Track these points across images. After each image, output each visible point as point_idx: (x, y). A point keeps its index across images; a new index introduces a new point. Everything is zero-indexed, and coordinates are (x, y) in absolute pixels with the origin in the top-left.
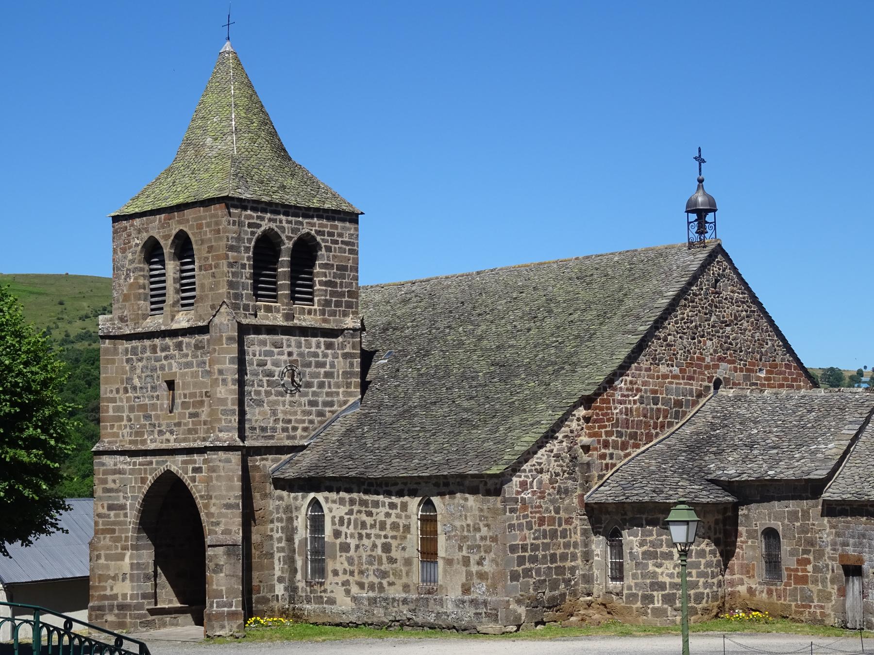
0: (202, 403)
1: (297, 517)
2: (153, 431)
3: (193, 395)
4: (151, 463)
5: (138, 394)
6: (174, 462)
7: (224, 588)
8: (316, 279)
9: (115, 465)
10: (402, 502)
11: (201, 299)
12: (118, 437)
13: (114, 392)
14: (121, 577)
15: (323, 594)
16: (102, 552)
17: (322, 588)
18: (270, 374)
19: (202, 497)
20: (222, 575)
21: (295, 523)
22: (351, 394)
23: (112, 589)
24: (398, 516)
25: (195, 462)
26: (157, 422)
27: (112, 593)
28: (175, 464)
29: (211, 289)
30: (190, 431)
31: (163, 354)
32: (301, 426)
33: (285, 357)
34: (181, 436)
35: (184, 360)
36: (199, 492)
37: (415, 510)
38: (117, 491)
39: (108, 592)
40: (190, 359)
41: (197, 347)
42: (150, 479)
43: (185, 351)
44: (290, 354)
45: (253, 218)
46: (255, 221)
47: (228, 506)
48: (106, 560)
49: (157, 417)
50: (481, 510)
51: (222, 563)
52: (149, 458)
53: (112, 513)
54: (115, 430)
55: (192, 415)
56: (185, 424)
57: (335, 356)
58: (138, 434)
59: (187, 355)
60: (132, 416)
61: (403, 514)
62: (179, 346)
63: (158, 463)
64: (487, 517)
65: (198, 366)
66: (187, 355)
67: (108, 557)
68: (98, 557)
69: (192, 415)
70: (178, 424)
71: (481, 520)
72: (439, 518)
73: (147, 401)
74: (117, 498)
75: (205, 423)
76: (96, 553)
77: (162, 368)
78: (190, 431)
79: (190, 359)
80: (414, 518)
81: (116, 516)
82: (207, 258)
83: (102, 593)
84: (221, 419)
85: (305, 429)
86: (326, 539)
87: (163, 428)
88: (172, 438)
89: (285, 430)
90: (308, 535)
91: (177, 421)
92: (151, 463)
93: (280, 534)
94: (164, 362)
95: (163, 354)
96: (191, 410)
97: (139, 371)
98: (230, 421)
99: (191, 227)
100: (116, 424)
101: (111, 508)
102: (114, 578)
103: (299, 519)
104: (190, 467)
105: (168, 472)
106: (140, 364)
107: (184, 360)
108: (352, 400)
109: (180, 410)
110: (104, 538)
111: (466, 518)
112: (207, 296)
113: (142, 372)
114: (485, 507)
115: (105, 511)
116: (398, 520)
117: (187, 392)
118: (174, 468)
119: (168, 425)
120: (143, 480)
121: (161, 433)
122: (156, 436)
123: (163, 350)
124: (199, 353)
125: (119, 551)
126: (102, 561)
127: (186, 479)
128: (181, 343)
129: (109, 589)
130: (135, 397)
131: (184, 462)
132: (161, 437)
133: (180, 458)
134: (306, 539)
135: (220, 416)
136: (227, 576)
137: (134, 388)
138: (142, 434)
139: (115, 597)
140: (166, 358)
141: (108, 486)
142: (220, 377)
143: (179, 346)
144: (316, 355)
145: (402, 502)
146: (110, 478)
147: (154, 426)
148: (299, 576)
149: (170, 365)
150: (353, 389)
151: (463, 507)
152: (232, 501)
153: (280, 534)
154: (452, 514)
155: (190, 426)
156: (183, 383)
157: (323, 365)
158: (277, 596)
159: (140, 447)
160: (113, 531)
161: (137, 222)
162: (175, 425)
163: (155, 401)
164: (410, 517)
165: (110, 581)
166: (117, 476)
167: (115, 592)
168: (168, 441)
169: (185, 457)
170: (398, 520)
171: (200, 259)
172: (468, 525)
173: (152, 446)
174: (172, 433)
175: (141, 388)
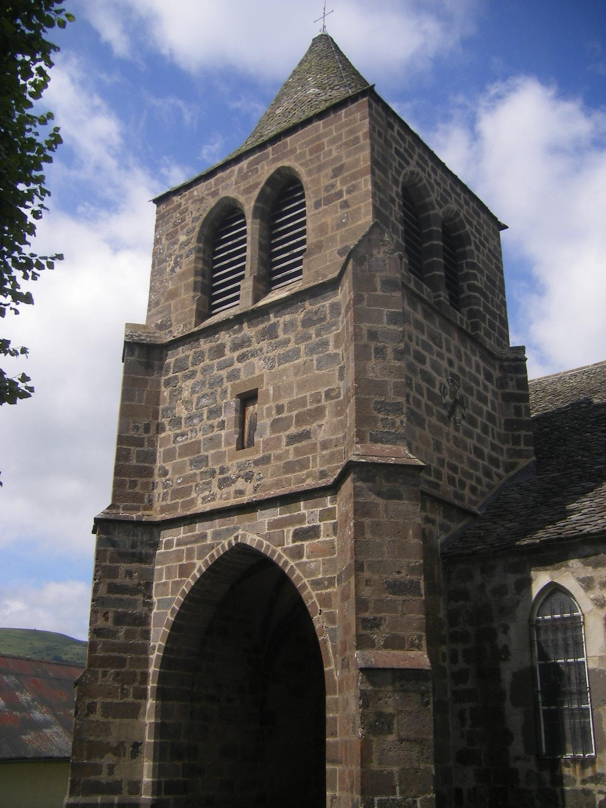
0: (318, 413)
1: (506, 629)
2: (209, 483)
3: (302, 402)
4: (204, 537)
5: (184, 429)
6: (252, 529)
7: (395, 769)
8: (465, 285)
9: (134, 546)
11: (319, 246)
12: (142, 501)
13: (141, 430)
14: (129, 749)
15: (590, 786)
16: (99, 700)
17: (589, 772)
18: (430, 380)
19: (316, 584)
20: (391, 738)
21: (501, 640)
22: (520, 454)
23: (111, 769)
25: (301, 519)
26: (217, 467)
27: (110, 779)
28: (254, 532)
29: (340, 225)
30: (289, 467)
31: (236, 354)
32: (468, 482)
33: (444, 364)
34: (268, 480)
35: (280, 351)
36: (312, 573)
38: (134, 591)
39: (104, 777)
40: (292, 346)
41: (307, 323)
42: (200, 565)
43: (282, 336)
44: (451, 363)
45: (401, 146)
46: (402, 150)
47: (396, 587)
48: (105, 714)
49: (220, 457)
51: (390, 710)
52: (199, 528)
53: (122, 630)
54: (137, 489)
55: (292, 439)
56: (279, 458)
57: (495, 394)
58: (177, 493)
59: (287, 342)
60: (168, 466)
62: (270, 333)
63: (217, 535)
65: (311, 351)
66: (287, 342)
67: (108, 710)
68: (91, 709)
69: (292, 439)
70: (265, 460)
73: (200, 436)
74: (133, 604)
75: (325, 445)
76: (88, 701)
77: (233, 376)
78: (289, 467)
79: (292, 346)
81: (128, 634)
82: (333, 186)
83: (92, 778)
84: (375, 419)
85: (473, 490)
86: (591, 665)
87: (231, 474)
88: (249, 487)
89: (451, 481)
90: (537, 663)
91: (261, 455)
92: (204, 537)
93: (462, 664)
94: (238, 365)
95: (236, 354)
96: (293, 430)
97: (186, 394)
98: (393, 424)
99: (297, 159)
100: (140, 481)
101: (120, 619)
102: (118, 750)
103: (512, 632)
104: (289, 531)
105: (242, 550)
106: (190, 383)
107: (280, 351)
108: (523, 463)
109: (268, 434)
110: (105, 674)
112: (332, 239)
113: (193, 392)
115: (110, 624)
117: (285, 401)
118: (252, 539)
119: (241, 467)
120: (184, 571)
121: (225, 483)
122: (215, 489)
123: (235, 348)
124: (312, 331)
125: (131, 699)
126: (97, 716)
127: (280, 555)
128: (274, 327)
129: (105, 771)
130: (177, 436)
131: (272, 525)
132: (225, 490)
133: (265, 517)
134: (533, 669)
135: (375, 413)
136: (401, 740)
137: (176, 422)
138: (185, 492)
139: (114, 788)
140: (241, 358)
141: (118, 581)
142: (373, 345)
143: (270, 333)
144: (477, 382)
146: (123, 567)
147: (213, 473)
148: (517, 747)
149: (252, 367)
150: (522, 447)
152: (405, 576)
153: (462, 664)
155: (291, 457)
156: (277, 389)
157: (483, 399)
158: (458, 792)
159: (180, 513)
160: (121, 662)
161: (197, 191)
162: (257, 463)
163: (216, 432)
165: (110, 755)
166: (135, 565)
167: (117, 776)
168: (240, 493)
169: (276, 514)
171: (316, 193)
173: (208, 507)
174: (248, 477)
175: (190, 418)
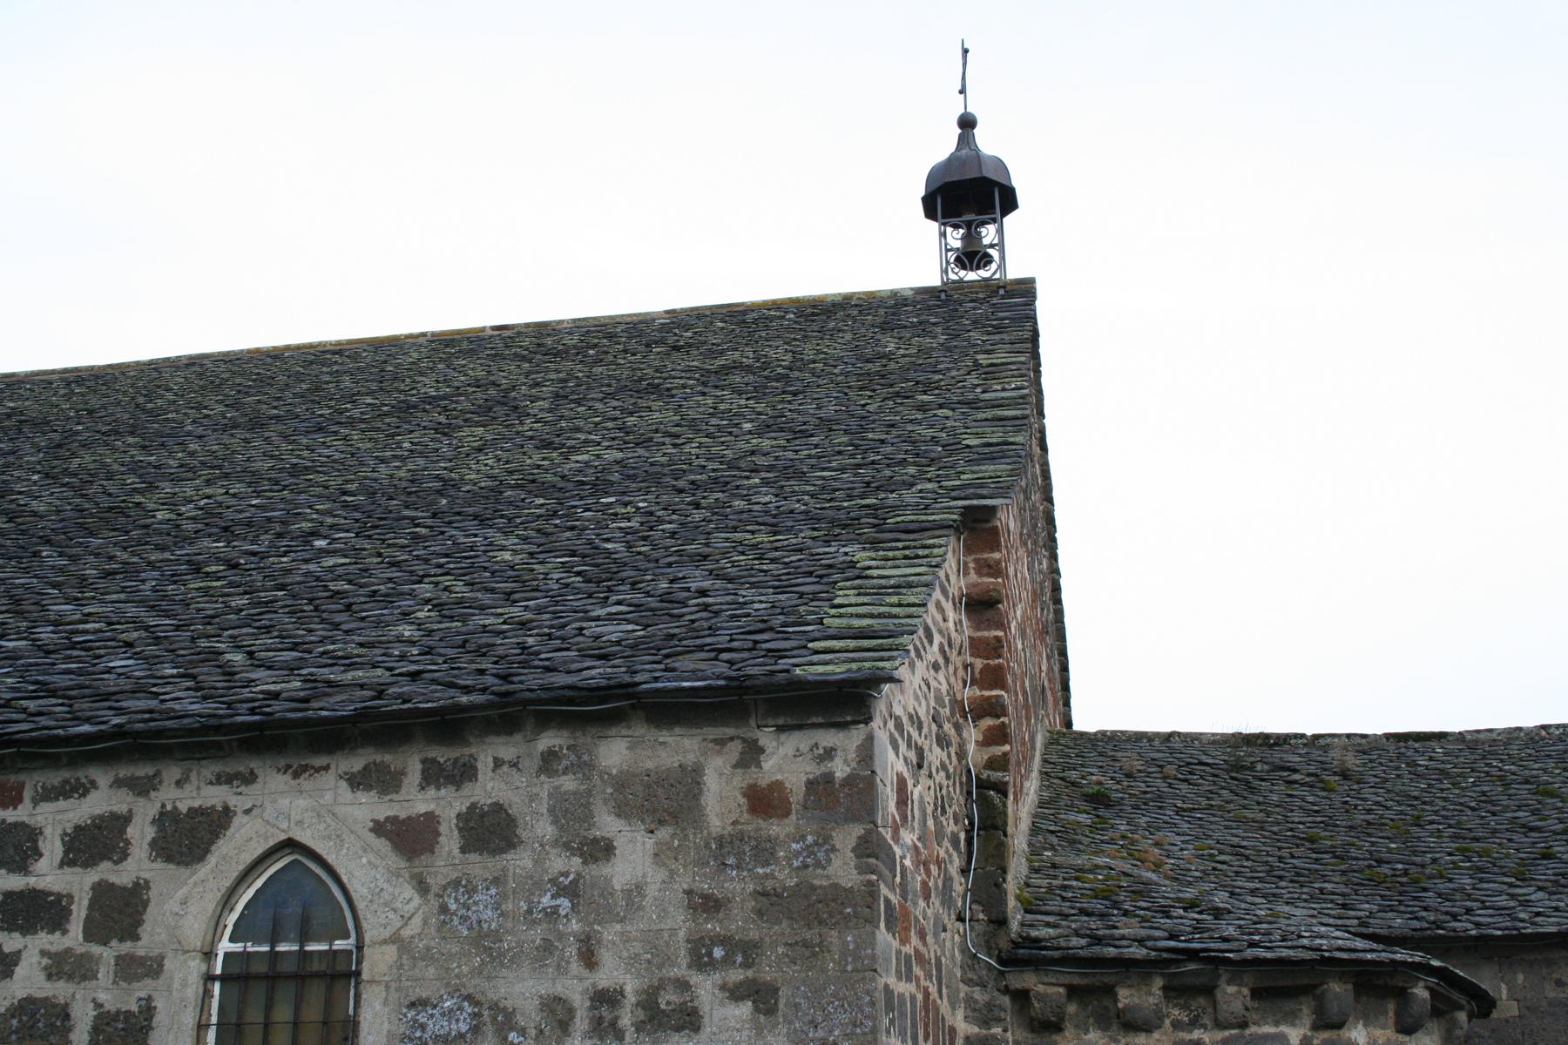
10: (102, 891)
24: (61, 966)
37: (194, 930)
50: (706, 905)
61: (107, 954)
64: (748, 951)
71: (701, 961)
72: (378, 962)
80: (185, 975)
111: (589, 959)
114: (737, 886)
116: (60, 990)
145: (102, 891)
151: (571, 890)
154: (485, 942)
164: (153, 968)
170: (60, 990)
172: (606, 998)
